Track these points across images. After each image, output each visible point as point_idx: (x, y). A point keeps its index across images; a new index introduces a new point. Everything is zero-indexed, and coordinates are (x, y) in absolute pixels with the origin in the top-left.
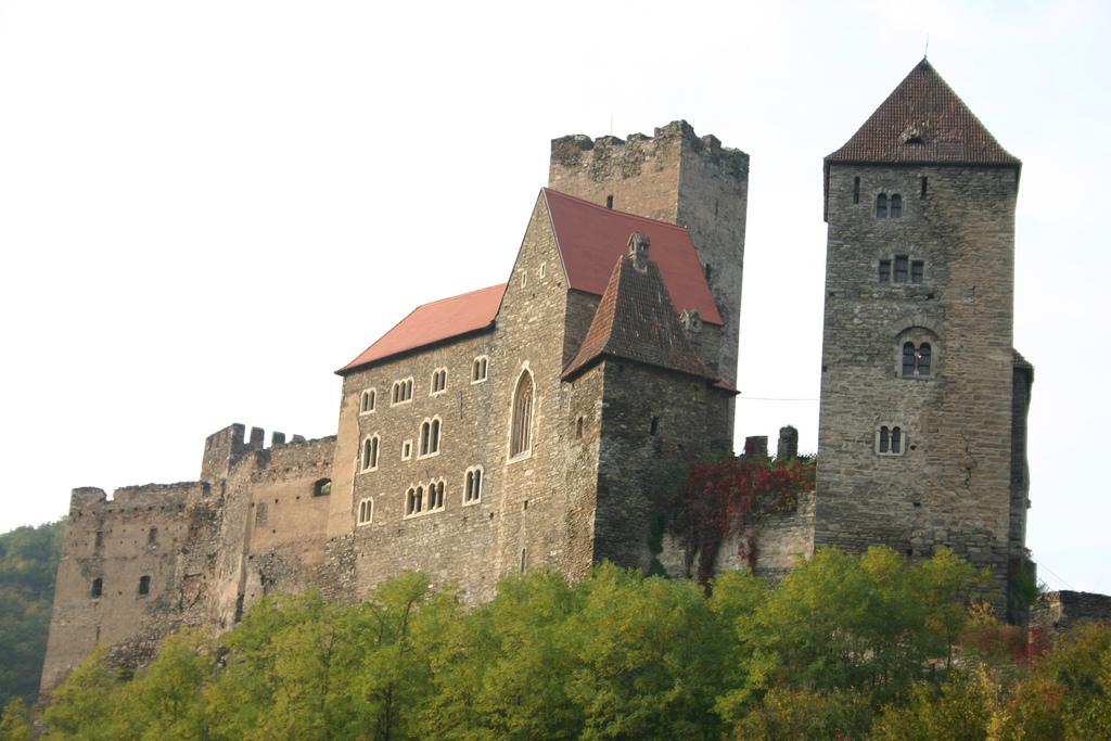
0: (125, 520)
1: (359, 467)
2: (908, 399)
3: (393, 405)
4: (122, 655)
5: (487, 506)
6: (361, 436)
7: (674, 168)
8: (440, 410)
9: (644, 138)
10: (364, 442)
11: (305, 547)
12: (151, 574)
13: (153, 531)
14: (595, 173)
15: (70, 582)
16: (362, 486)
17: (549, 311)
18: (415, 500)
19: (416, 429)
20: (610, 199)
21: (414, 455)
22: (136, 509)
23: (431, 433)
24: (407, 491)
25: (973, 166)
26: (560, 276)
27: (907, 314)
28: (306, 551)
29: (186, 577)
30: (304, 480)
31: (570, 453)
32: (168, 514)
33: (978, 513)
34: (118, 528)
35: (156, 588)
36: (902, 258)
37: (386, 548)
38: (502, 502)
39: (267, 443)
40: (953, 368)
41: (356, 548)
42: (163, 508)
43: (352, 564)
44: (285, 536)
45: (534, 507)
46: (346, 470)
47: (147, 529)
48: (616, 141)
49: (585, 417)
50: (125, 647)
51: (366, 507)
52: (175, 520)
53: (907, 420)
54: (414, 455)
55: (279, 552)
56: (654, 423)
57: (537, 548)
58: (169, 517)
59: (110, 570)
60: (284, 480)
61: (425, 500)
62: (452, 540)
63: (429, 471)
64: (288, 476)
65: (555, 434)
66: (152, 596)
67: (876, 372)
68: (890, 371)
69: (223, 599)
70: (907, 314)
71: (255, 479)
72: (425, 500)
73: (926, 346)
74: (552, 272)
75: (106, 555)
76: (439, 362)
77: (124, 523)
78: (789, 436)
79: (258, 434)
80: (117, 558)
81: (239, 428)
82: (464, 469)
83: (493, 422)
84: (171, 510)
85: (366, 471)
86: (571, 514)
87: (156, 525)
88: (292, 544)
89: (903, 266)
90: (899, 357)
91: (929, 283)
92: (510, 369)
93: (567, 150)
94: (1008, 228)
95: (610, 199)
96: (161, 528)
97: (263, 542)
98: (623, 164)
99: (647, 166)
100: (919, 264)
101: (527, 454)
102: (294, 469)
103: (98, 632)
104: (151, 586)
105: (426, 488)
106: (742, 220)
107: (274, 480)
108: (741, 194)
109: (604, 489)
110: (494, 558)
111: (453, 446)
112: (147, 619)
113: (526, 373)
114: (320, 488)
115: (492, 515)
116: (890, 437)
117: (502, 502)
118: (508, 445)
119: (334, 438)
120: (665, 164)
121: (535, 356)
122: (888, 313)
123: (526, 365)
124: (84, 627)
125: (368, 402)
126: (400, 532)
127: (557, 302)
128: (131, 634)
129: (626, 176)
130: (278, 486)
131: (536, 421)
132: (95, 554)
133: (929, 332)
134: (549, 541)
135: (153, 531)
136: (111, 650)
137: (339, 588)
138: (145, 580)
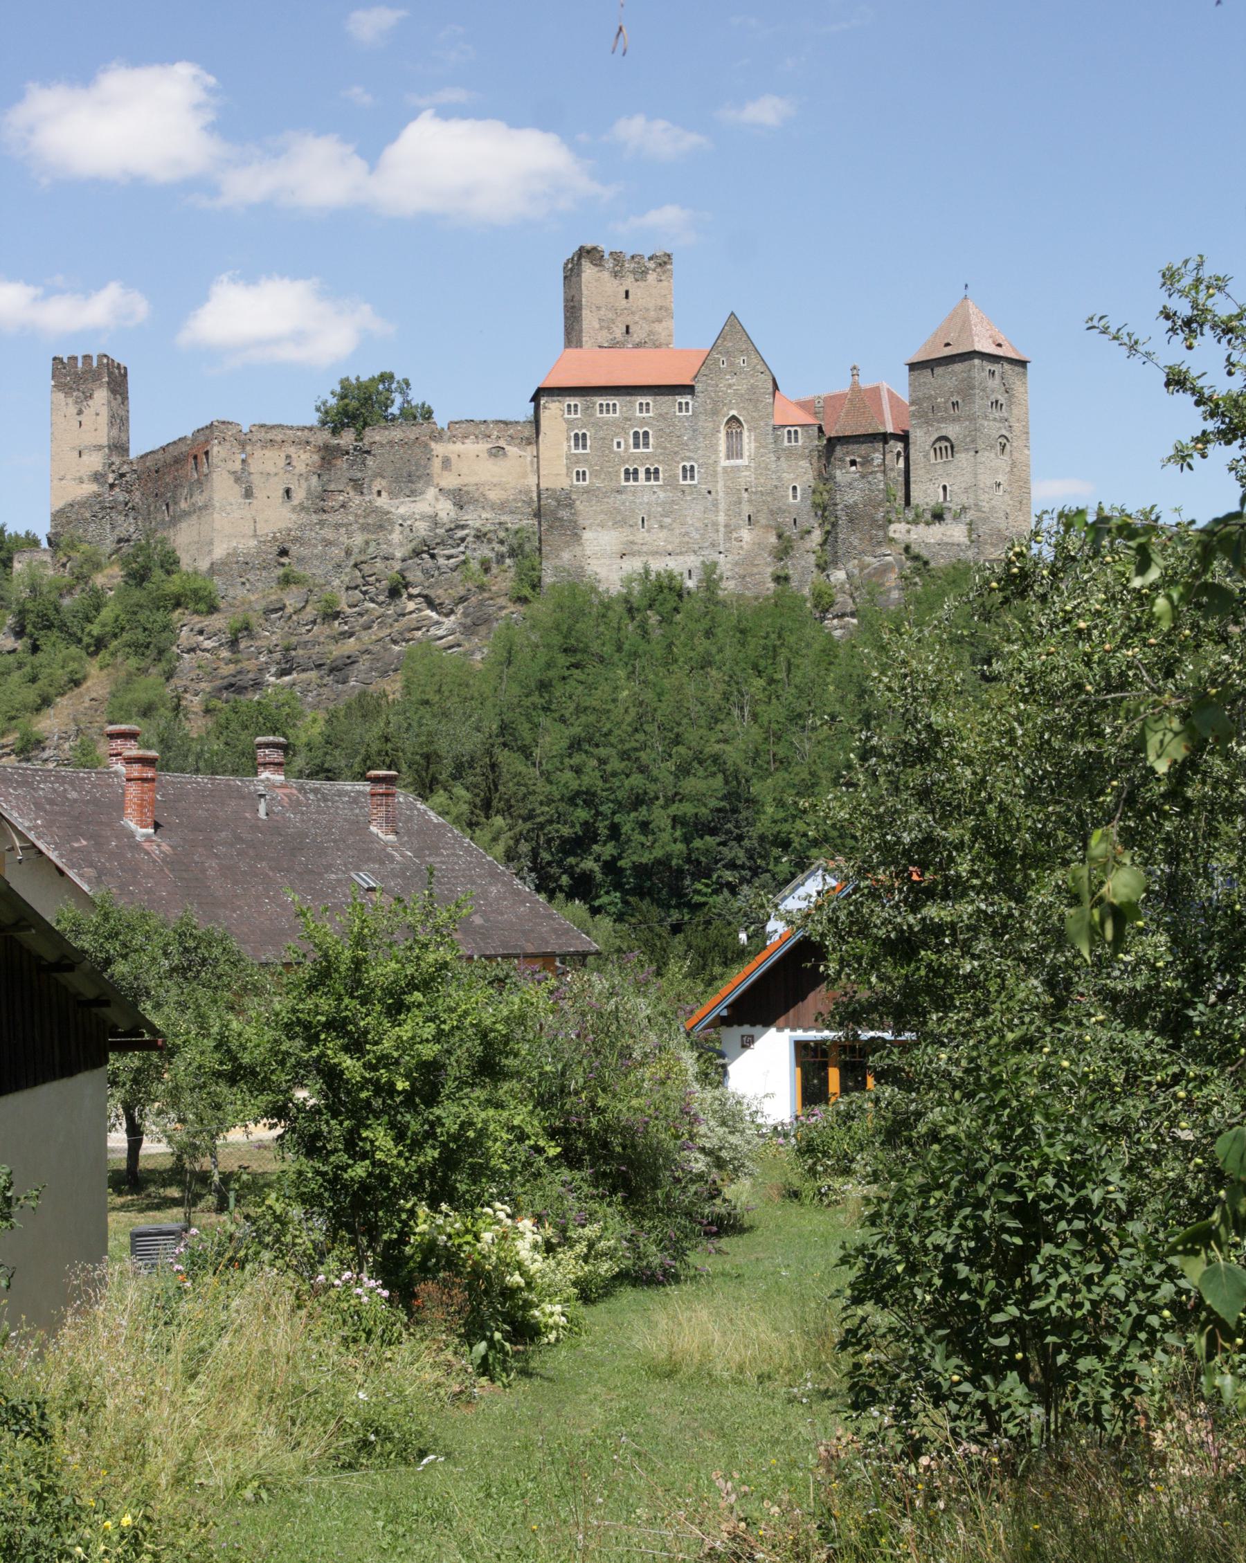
0: (263, 447)
6: (569, 430)
13: (288, 457)
14: (616, 275)
15: (222, 488)
18: (632, 474)
20: (627, 293)
21: (627, 449)
23: (641, 439)
34: (258, 453)
35: (299, 495)
38: (720, 486)
43: (571, 506)
44: (472, 480)
47: (283, 455)
54: (627, 449)
59: (256, 480)
61: (642, 475)
66: (295, 502)
72: (642, 475)
91: (1005, 414)
99: (652, 277)
104: (293, 495)
112: (294, 517)
117: (720, 486)
118: (722, 454)
123: (733, 412)
128: (281, 525)
130: (458, 447)
135: (288, 457)
137: (561, 520)
138: (288, 492)
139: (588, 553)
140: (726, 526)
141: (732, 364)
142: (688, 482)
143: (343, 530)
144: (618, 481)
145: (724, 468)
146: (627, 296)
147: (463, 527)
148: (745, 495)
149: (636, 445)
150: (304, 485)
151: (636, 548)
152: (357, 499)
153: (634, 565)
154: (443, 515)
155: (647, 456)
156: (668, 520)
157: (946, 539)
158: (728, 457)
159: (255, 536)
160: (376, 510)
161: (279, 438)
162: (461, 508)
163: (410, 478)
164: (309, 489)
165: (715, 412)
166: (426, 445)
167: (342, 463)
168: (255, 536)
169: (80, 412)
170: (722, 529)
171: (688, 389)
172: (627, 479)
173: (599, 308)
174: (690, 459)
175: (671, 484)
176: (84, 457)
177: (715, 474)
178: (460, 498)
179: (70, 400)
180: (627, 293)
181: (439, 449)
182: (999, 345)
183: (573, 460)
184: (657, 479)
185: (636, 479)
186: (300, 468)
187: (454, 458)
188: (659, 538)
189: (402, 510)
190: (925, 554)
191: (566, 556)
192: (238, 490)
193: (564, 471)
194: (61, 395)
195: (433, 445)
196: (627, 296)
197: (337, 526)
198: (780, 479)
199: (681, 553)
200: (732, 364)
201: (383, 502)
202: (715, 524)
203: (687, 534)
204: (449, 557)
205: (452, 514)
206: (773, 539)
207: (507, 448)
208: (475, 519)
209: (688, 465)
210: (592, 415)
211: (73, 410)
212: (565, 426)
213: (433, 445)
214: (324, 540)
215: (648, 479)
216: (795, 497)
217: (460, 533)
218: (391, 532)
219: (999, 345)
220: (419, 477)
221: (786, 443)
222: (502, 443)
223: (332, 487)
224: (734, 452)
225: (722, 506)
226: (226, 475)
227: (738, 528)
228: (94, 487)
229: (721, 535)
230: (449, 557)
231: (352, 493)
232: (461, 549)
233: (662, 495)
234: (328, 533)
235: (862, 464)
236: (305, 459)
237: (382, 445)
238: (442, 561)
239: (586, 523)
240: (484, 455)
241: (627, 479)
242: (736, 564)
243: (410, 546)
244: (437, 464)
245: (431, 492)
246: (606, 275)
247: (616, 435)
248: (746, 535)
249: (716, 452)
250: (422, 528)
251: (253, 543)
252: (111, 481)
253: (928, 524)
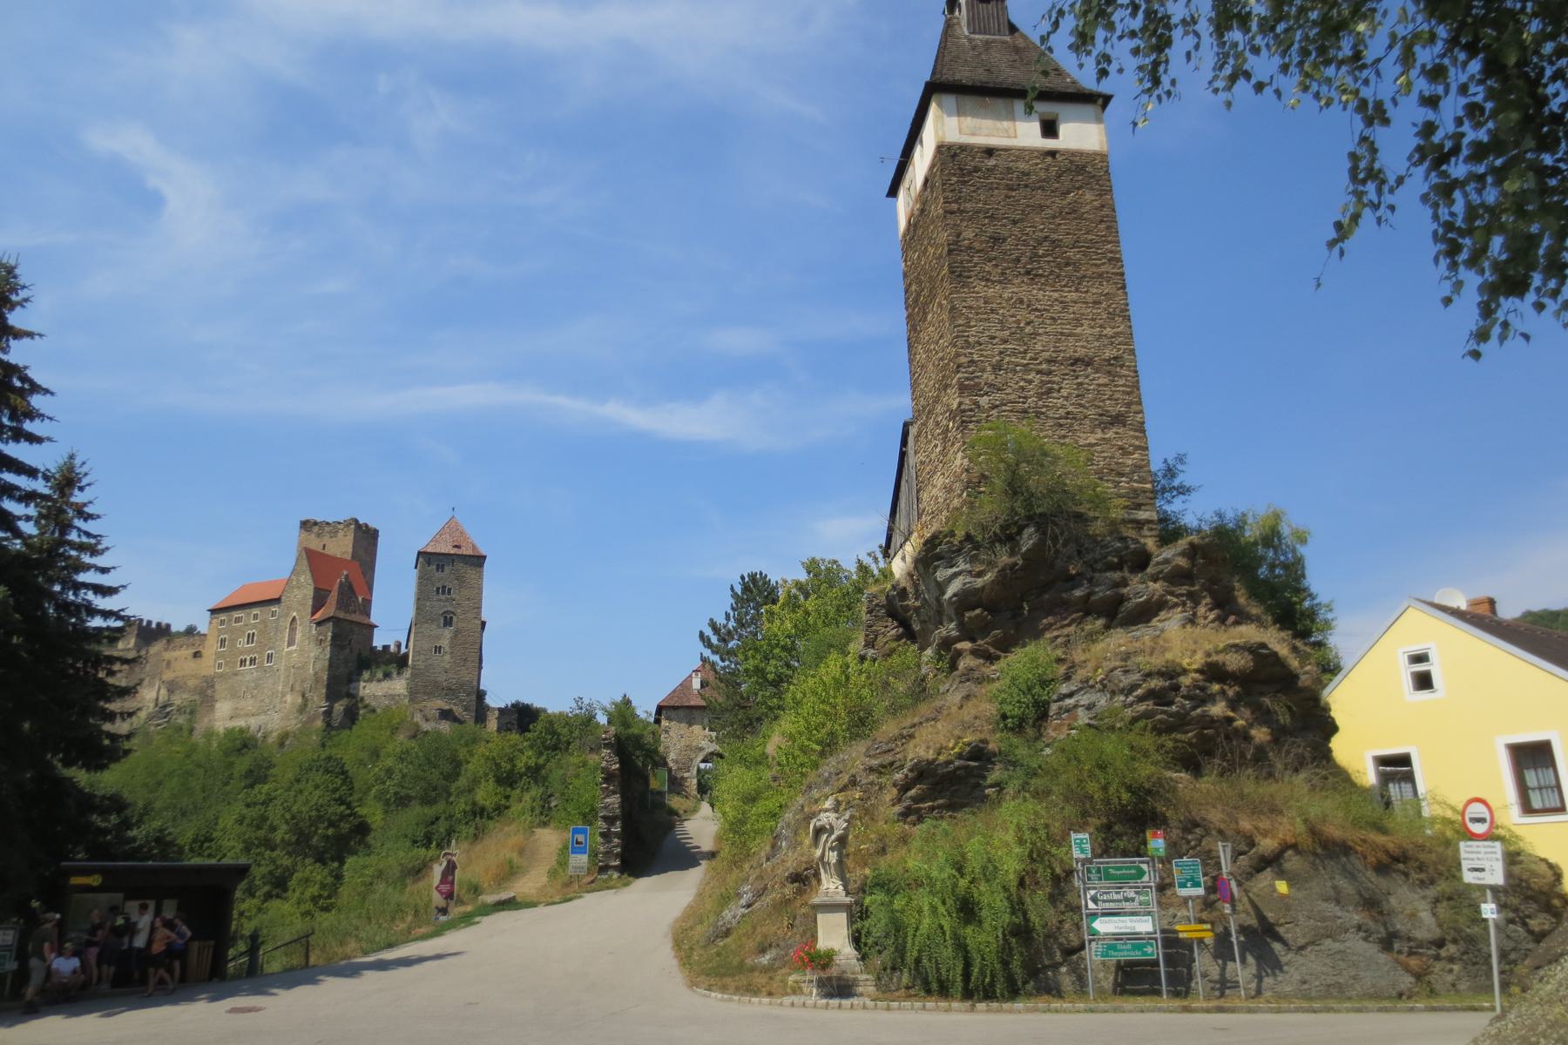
2: (445, 637)
7: (351, 537)
8: (254, 626)
9: (340, 523)
14: (319, 535)
16: (218, 655)
17: (305, 595)
18: (243, 662)
20: (324, 546)
23: (251, 638)
25: (470, 556)
26: (310, 581)
27: (445, 606)
31: (314, 651)
33: (466, 676)
36: (444, 587)
39: (154, 626)
40: (461, 625)
43: (212, 686)
46: (211, 649)
48: (328, 524)
51: (220, 666)
53: (445, 643)
56: (350, 641)
57: (298, 684)
61: (248, 663)
62: (260, 679)
63: (250, 651)
67: (434, 627)
68: (439, 627)
69: (148, 697)
70: (445, 606)
71: (166, 650)
72: (248, 663)
73: (451, 618)
74: (306, 579)
76: (256, 611)
78: (399, 645)
79: (149, 622)
81: (141, 620)
86: (316, 673)
89: (444, 590)
90: (442, 621)
92: (287, 615)
93: (306, 525)
94: (481, 577)
95: (324, 546)
97: (168, 676)
98: (330, 532)
99: (341, 534)
100: (450, 589)
101: (294, 648)
105: (248, 658)
106: (375, 555)
108: (375, 545)
109: (331, 666)
113: (294, 618)
114: (197, 655)
116: (438, 649)
117: (282, 668)
119: (205, 635)
121: (298, 611)
122: (438, 606)
123: (295, 614)
125: (222, 622)
126: (236, 675)
127: (309, 591)
130: (176, 654)
131: (298, 636)
133: (453, 613)
134: (303, 681)
137: (207, 696)
147: (171, 705)
156: (255, 692)
157: (390, 692)
162: (173, 692)
171: (277, 601)
174: (270, 648)
175: (261, 667)
178: (172, 688)
181: (167, 655)
182: (456, 546)
188: (249, 705)
190: (374, 704)
191: (206, 720)
202: (277, 692)
203: (262, 701)
204: (158, 725)
206: (300, 700)
217: (168, 709)
219: (456, 546)
225: (282, 680)
233: (255, 674)
240: (190, 657)
247: (241, 637)
248: (289, 698)
253: (379, 681)
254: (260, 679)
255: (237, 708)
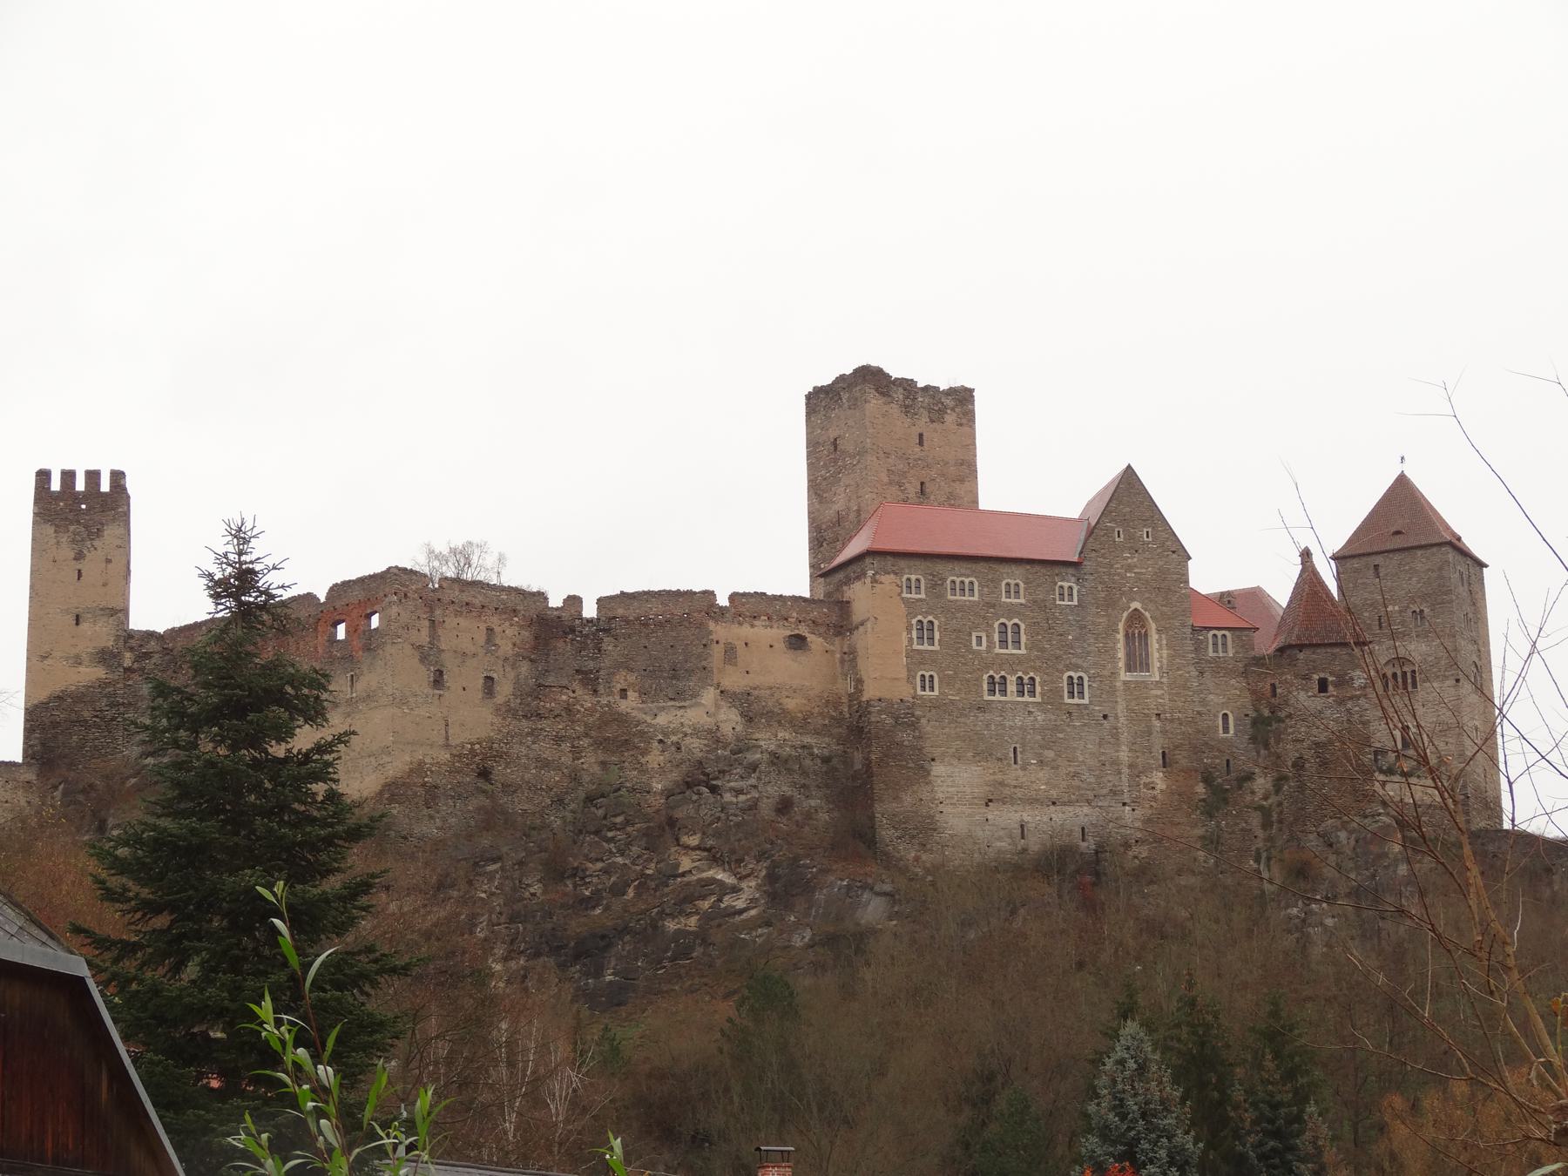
0: (458, 614)
1: (911, 639)
3: (950, 597)
4: (477, 755)
5: (1097, 708)
6: (911, 615)
10: (914, 621)
11: (787, 694)
12: (495, 675)
13: (490, 630)
19: (992, 626)
20: (921, 435)
22: (467, 604)
24: (985, 677)
28: (787, 697)
29: (540, 685)
30: (775, 630)
32: (504, 617)
34: (451, 621)
37: (962, 720)
38: (1121, 708)
41: (918, 713)
42: (496, 609)
43: (914, 725)
45: (1172, 721)
47: (483, 627)
49: (1330, 679)
50: (477, 746)
51: (927, 682)
52: (511, 625)
55: (756, 693)
58: (505, 620)
60: (752, 626)
61: (1012, 687)
62: (1056, 729)
64: (756, 623)
65: (1192, 668)
66: (500, 699)
72: (1012, 687)
75: (443, 647)
77: (456, 616)
80: (455, 651)
82: (1062, 672)
83: (1092, 641)
84: (505, 613)
85: (920, 647)
87: (493, 626)
88: (771, 688)
96: (497, 629)
97: (733, 680)
99: (950, 418)
102: (763, 618)
103: (447, 725)
107: (740, 624)
110: (1117, 751)
111: (1043, 650)
115: (1105, 717)
117: (1121, 708)
118: (1121, 664)
120: (964, 421)
123: (1136, 605)
124: (429, 717)
128: (483, 732)
129: (932, 421)
132: (430, 643)
135: (490, 630)
136: (463, 747)
137: (900, 744)
139: (940, 796)
140: (1131, 766)
141: (1131, 537)
142: (1076, 701)
143: (566, 746)
144: (980, 694)
145: (1125, 683)
146: (921, 443)
148: (1157, 723)
149: (1003, 643)
150: (511, 675)
151: (1007, 791)
152: (588, 701)
153: (1007, 817)
154: (726, 729)
155: (1019, 660)
156: (1050, 754)
158: (1129, 668)
159: (447, 746)
160: (621, 719)
161: (477, 602)
163: (675, 674)
164: (517, 681)
165: (1110, 603)
166: (701, 626)
167: (563, 647)
168: (447, 746)
169: (79, 556)
170: (1125, 770)
172: (992, 692)
173: (887, 455)
174: (1076, 668)
176: (84, 626)
177: (1112, 691)
178: (750, 706)
179: (64, 539)
180: (921, 435)
183: (917, 660)
184: (1032, 693)
185: (1004, 692)
186: (506, 648)
187: (740, 645)
188: (1039, 780)
189: (662, 720)
191: (908, 799)
192: (425, 674)
193: (904, 674)
194: (50, 530)
195: (712, 625)
196: (921, 443)
197: (558, 740)
198: (1203, 702)
199: (1070, 803)
200: (1131, 537)
201: (630, 705)
202: (1115, 762)
203: (1076, 775)
204: (739, 792)
205: (739, 728)
207: (810, 638)
208: (768, 739)
209: (1075, 675)
210: (941, 596)
211: (67, 552)
212: (903, 609)
213: (712, 625)
214: (538, 759)
215: (1021, 693)
216: (1226, 730)
218: (645, 753)
220: (691, 672)
221: (1211, 654)
222: (803, 630)
223: (550, 680)
224: (1137, 661)
226: (408, 649)
227: (1147, 770)
228: (100, 672)
229: (1125, 778)
230: (739, 792)
231: (579, 692)
232: (753, 781)
234: (545, 749)
235: (1337, 685)
236: (510, 636)
237: (627, 622)
238: (728, 797)
239: (937, 752)
240: (781, 646)
241: (992, 692)
242: (1148, 821)
243: (675, 776)
244: (717, 652)
245: (709, 696)
246: (895, 410)
247: (976, 627)
248: (1159, 779)
249: (1114, 658)
250: (695, 745)
251: (445, 756)
252: (127, 663)
254: (1056, 729)
255: (1002, 784)
